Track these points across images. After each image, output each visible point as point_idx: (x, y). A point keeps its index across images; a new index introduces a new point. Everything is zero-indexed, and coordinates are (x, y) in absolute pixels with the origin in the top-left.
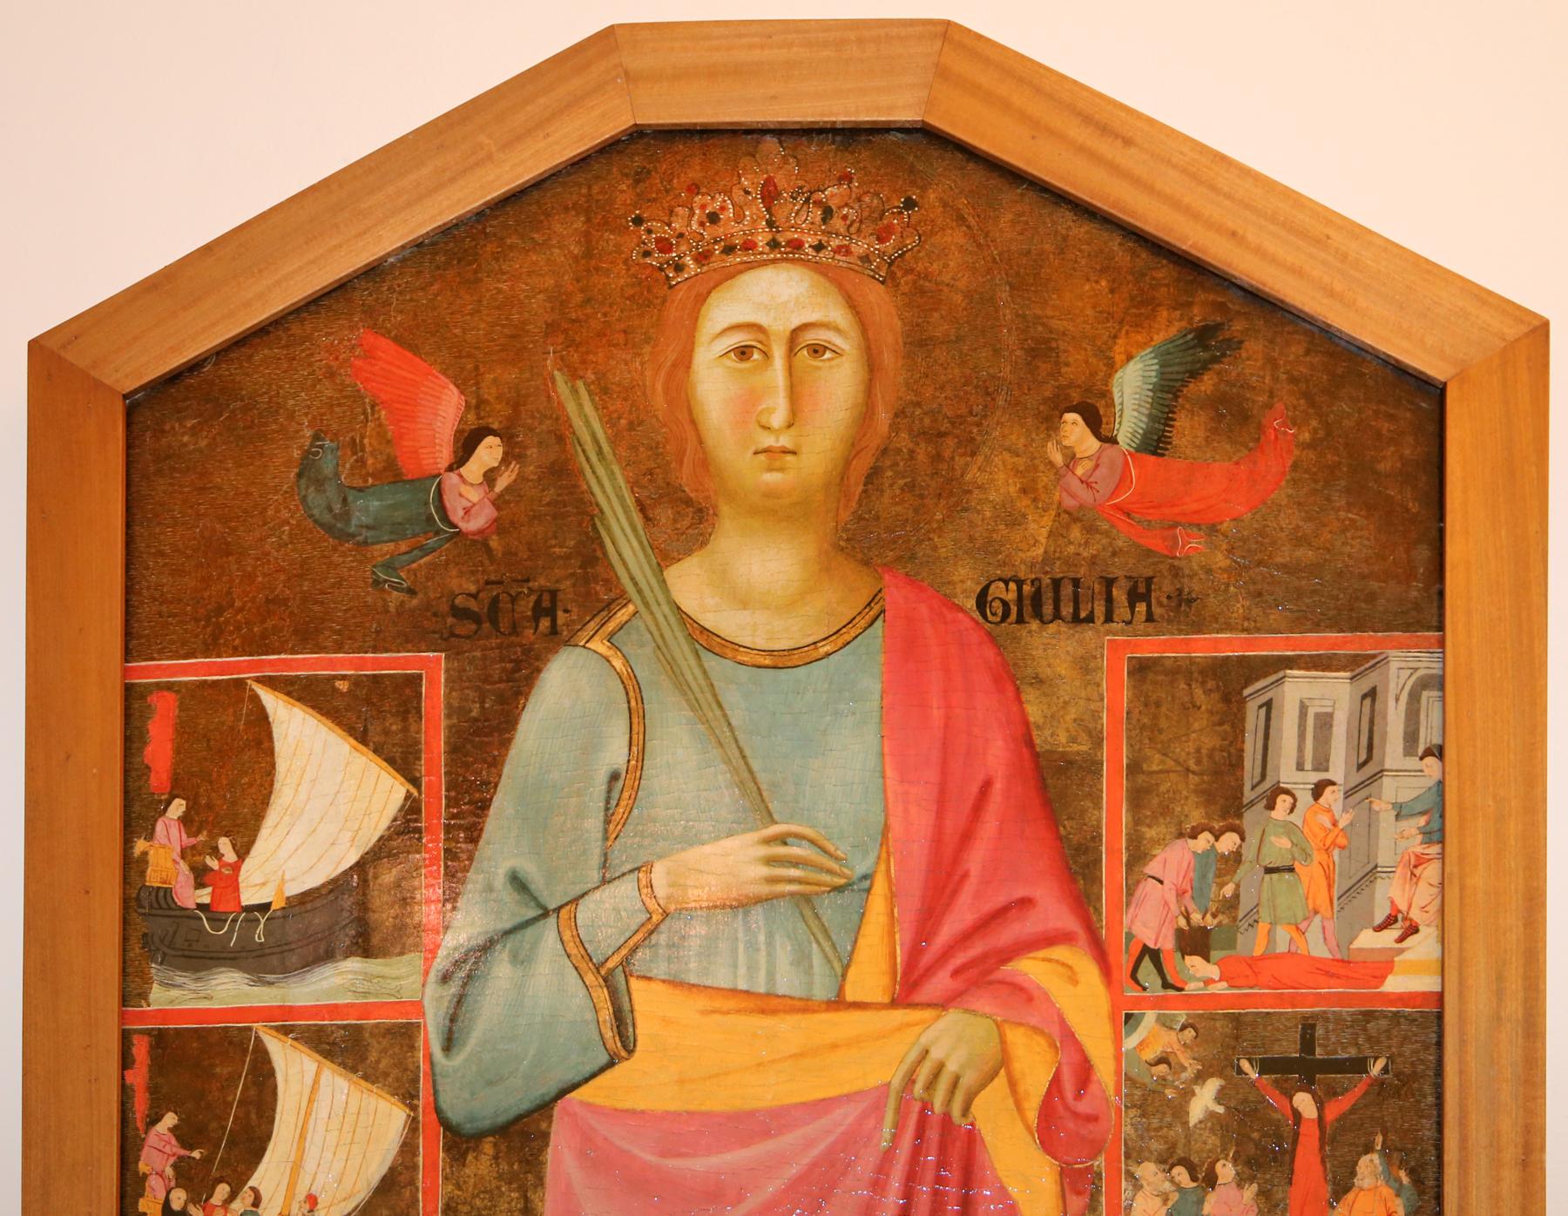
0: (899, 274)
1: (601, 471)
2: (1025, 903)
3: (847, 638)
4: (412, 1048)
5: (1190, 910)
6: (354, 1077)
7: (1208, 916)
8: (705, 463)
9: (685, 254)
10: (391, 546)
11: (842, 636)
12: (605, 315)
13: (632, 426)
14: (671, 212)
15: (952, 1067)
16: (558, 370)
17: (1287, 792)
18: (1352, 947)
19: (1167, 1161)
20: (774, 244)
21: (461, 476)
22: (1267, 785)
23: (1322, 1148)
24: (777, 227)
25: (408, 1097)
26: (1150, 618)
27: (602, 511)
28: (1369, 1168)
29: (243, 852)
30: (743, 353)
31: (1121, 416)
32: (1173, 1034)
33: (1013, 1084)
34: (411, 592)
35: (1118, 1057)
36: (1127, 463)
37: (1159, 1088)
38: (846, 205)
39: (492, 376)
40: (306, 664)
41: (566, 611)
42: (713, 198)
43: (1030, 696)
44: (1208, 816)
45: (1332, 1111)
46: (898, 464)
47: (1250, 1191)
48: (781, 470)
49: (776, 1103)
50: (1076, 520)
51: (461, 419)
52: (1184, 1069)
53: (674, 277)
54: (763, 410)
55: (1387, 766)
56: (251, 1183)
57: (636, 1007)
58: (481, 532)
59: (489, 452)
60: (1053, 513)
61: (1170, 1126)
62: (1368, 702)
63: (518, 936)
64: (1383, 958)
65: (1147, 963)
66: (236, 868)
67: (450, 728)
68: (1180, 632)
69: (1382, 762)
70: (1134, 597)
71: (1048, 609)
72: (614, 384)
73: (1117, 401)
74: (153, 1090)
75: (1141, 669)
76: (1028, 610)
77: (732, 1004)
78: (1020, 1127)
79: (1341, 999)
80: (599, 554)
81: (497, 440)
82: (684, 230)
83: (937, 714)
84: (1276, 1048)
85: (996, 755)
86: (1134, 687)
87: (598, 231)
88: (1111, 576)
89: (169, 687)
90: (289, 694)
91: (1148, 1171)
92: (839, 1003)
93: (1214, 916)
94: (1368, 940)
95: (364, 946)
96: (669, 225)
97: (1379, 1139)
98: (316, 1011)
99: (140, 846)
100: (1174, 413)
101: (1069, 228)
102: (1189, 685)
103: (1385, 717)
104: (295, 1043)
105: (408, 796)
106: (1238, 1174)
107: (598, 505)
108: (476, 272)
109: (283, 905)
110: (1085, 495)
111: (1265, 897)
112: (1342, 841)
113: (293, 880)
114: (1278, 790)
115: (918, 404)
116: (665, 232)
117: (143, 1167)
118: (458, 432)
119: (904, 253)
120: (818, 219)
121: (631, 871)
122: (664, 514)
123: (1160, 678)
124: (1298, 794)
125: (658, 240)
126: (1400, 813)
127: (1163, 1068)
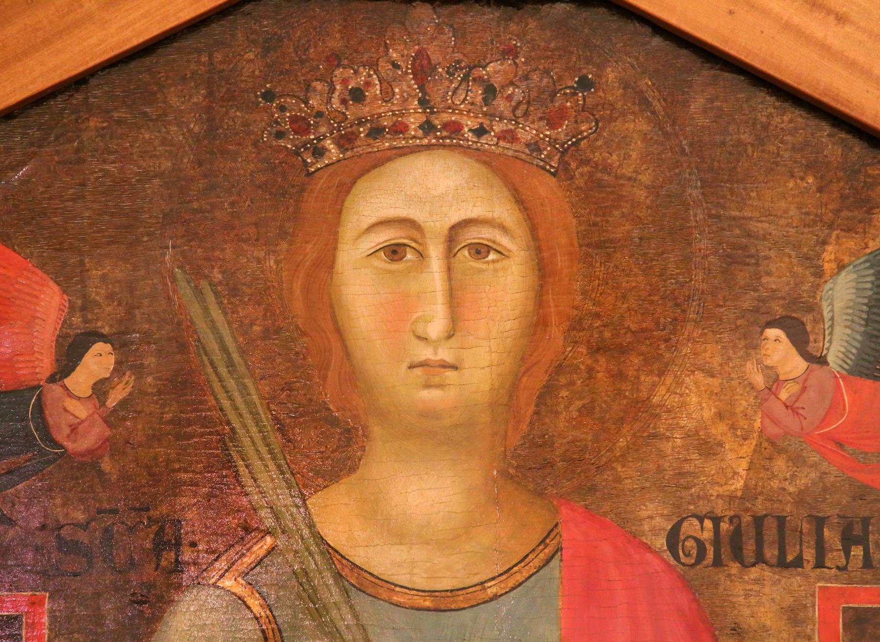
9: (325, 137)
12: (232, 204)
13: (266, 334)
14: (308, 87)
16: (178, 268)
20: (428, 127)
24: (432, 108)
30: (394, 252)
39: (100, 273)
42: (356, 72)
48: (440, 386)
51: (65, 322)
53: (313, 164)
54: (419, 318)
72: (244, 284)
81: (109, 348)
87: (222, 107)
108: (78, 150)
116: (301, 110)
118: (61, 338)
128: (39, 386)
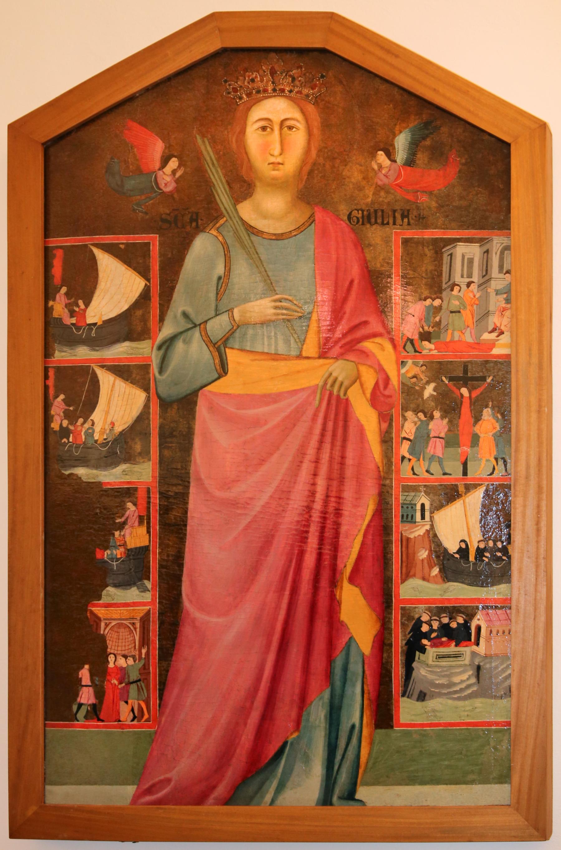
0: (319, 101)
1: (214, 170)
2: (366, 323)
3: (302, 229)
4: (148, 373)
5: (424, 326)
6: (127, 383)
7: (430, 328)
8: (251, 167)
10: (138, 197)
11: (300, 229)
12: (214, 114)
13: (224, 154)
14: (238, 79)
15: (340, 379)
17: (458, 285)
18: (481, 338)
19: (416, 411)
20: (274, 90)
21: (163, 172)
22: (451, 282)
23: (470, 407)
25: (146, 389)
26: (409, 224)
27: (214, 185)
28: (487, 413)
29: (87, 305)
31: (398, 153)
32: (418, 368)
33: (362, 385)
34: (146, 213)
35: (399, 375)
36: (400, 170)
37: (413, 386)
38: (300, 76)
40: (109, 239)
41: (202, 220)
43: (366, 250)
44: (430, 293)
45: (474, 395)
46: (319, 168)
47: (446, 421)
48: (278, 170)
49: (278, 391)
50: (383, 189)
52: (422, 380)
53: (239, 102)
55: (493, 277)
56: (91, 418)
57: (228, 358)
58: (171, 192)
59: (173, 163)
60: (374, 186)
61: (417, 399)
62: (486, 254)
63: (185, 334)
64: (492, 342)
65: (409, 343)
66: (85, 311)
67: (160, 261)
68: (420, 229)
69: (491, 275)
70: (403, 217)
71: (373, 220)
73: (396, 147)
74: (56, 386)
75: (406, 242)
76: (366, 220)
77: (263, 357)
78: (364, 399)
79: (477, 356)
80: (213, 199)
82: (242, 85)
83: (334, 256)
84: (455, 373)
85: (355, 271)
86: (404, 248)
88: (395, 209)
89: (61, 247)
90: (102, 249)
91: (409, 414)
92: (300, 357)
93: (433, 327)
94: (486, 336)
95: (130, 337)
96: (237, 83)
97: (490, 403)
98: (113, 360)
99: (51, 303)
100: (416, 152)
101: (379, 86)
102: (423, 248)
103: (492, 260)
104: (106, 371)
105: (146, 285)
106: (441, 415)
107: (212, 182)
109: (101, 323)
110: (386, 180)
111: (450, 321)
112: (477, 302)
113: (105, 315)
114: (455, 285)
115: (326, 148)
116: (235, 85)
117: (52, 412)
119: (321, 94)
120: (290, 81)
121: (226, 311)
122: (236, 186)
123: (413, 245)
124: (462, 286)
125: (233, 88)
126: (498, 293)
127: (415, 379)
128: (155, 172)
